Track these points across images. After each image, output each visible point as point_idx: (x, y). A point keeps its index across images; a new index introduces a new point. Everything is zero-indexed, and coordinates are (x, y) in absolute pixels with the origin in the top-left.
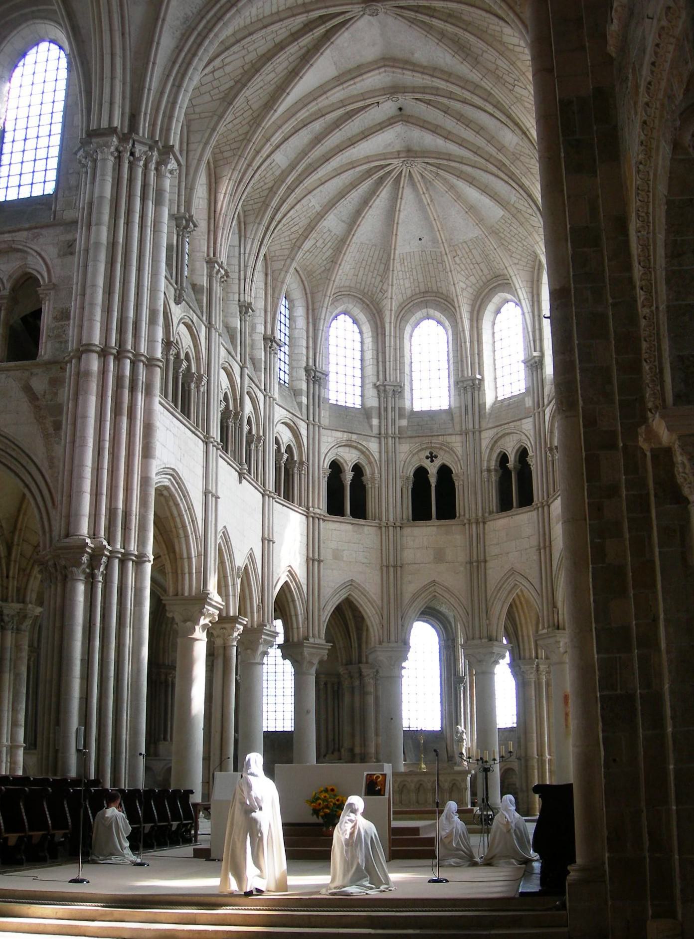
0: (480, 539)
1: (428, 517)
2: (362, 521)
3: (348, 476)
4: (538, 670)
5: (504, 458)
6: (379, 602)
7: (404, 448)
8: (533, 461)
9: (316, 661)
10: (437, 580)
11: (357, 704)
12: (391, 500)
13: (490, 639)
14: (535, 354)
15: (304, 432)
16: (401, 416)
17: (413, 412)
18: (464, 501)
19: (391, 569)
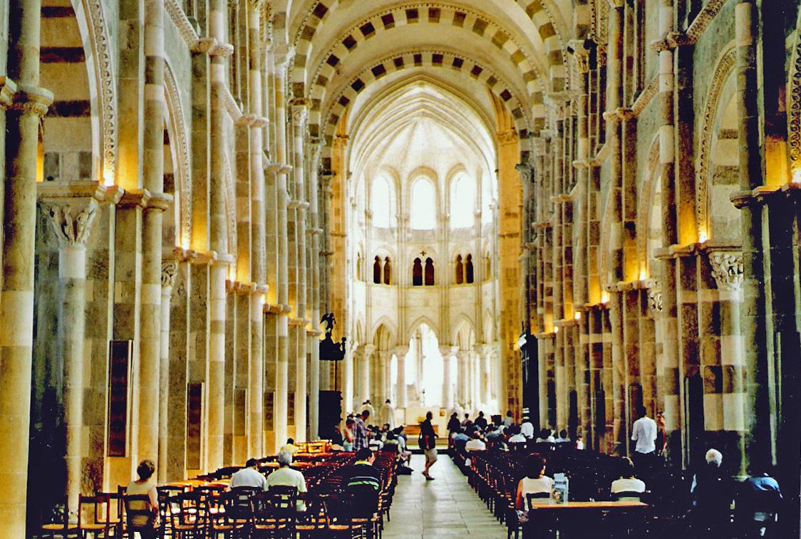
0: (447, 296)
1: (421, 284)
2: (388, 286)
3: (383, 263)
4: (469, 356)
5: (459, 258)
6: (397, 325)
7: (410, 248)
8: (474, 261)
9: (370, 353)
10: (425, 315)
11: (377, 370)
12: (403, 275)
13: (451, 345)
14: (478, 211)
15: (364, 246)
16: (409, 232)
17: (414, 231)
18: (438, 275)
19: (403, 309)
